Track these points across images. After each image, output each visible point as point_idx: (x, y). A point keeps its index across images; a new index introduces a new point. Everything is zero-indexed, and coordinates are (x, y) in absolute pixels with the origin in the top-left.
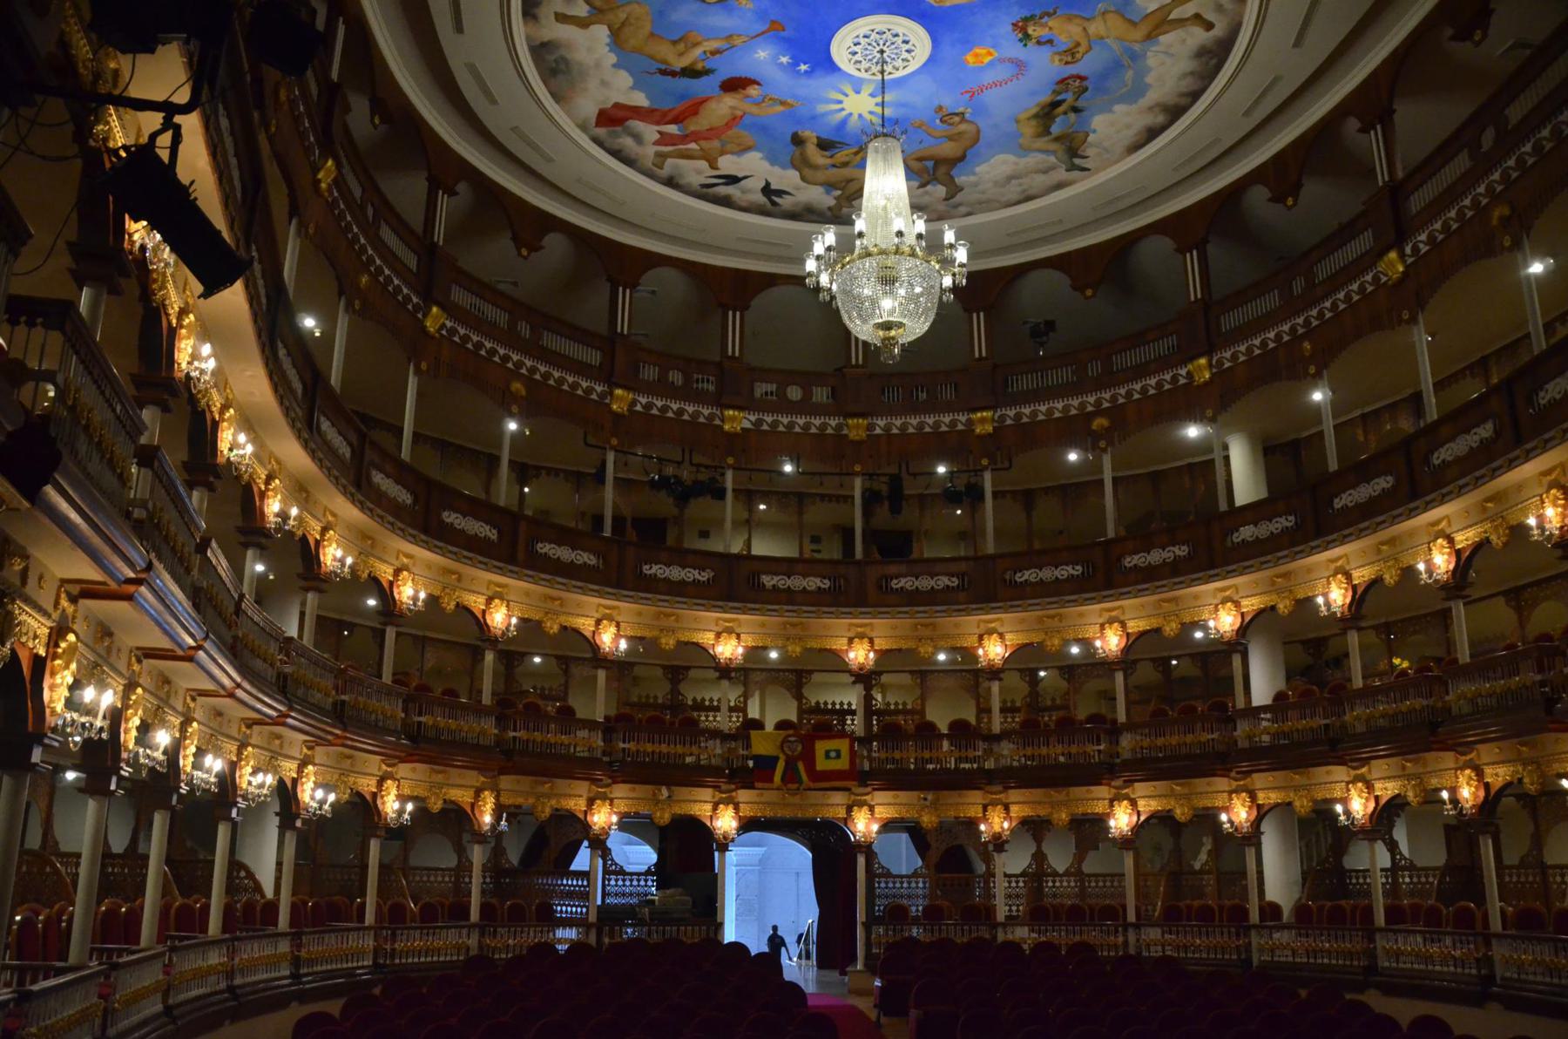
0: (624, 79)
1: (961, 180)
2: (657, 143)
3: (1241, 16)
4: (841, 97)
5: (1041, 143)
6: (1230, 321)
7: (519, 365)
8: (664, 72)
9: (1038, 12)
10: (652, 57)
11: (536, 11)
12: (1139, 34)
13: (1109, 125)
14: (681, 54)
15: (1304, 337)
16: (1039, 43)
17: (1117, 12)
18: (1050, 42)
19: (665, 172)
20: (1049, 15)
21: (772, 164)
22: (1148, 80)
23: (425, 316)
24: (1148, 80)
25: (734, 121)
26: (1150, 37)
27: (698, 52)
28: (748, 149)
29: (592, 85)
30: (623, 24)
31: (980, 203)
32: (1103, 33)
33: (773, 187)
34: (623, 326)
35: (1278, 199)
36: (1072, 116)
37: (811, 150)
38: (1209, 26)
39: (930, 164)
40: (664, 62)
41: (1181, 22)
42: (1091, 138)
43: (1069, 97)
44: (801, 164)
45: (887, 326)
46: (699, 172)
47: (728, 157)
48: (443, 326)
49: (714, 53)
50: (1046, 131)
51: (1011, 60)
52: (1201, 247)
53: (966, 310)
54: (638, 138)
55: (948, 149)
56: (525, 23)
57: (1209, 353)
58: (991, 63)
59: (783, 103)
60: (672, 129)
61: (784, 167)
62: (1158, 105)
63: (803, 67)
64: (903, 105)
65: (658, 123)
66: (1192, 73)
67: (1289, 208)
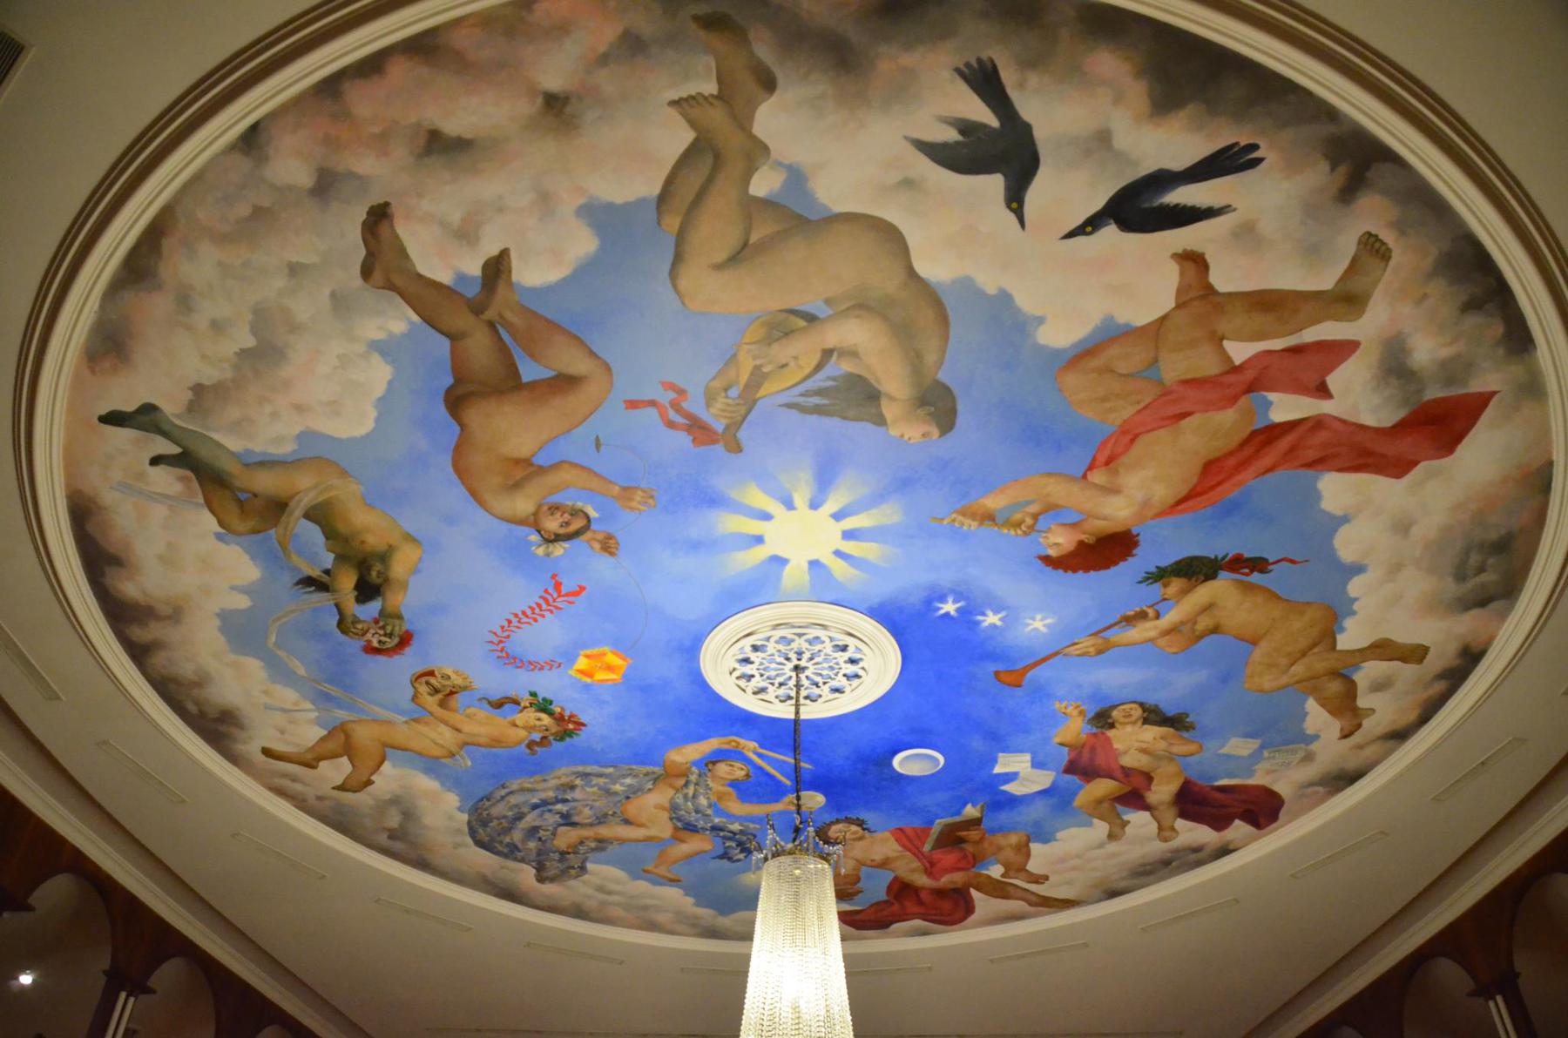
2: (1342, 350)
4: (850, 547)
9: (557, 746)
10: (1273, 596)
14: (1208, 608)
17: (437, 758)
19: (1372, 214)
25: (1110, 456)
27: (1172, 617)
28: (1084, 355)
29: (1429, 525)
30: (1304, 654)
33: (993, 185)
37: (894, 381)
39: (530, 371)
40: (1250, 588)
42: (209, 522)
44: (919, 309)
46: (1247, 234)
47: (1142, 317)
49: (1142, 616)
50: (321, 515)
54: (1395, 366)
55: (514, 430)
59: (989, 517)
60: (1284, 407)
61: (966, 285)
63: (950, 607)
64: (696, 546)
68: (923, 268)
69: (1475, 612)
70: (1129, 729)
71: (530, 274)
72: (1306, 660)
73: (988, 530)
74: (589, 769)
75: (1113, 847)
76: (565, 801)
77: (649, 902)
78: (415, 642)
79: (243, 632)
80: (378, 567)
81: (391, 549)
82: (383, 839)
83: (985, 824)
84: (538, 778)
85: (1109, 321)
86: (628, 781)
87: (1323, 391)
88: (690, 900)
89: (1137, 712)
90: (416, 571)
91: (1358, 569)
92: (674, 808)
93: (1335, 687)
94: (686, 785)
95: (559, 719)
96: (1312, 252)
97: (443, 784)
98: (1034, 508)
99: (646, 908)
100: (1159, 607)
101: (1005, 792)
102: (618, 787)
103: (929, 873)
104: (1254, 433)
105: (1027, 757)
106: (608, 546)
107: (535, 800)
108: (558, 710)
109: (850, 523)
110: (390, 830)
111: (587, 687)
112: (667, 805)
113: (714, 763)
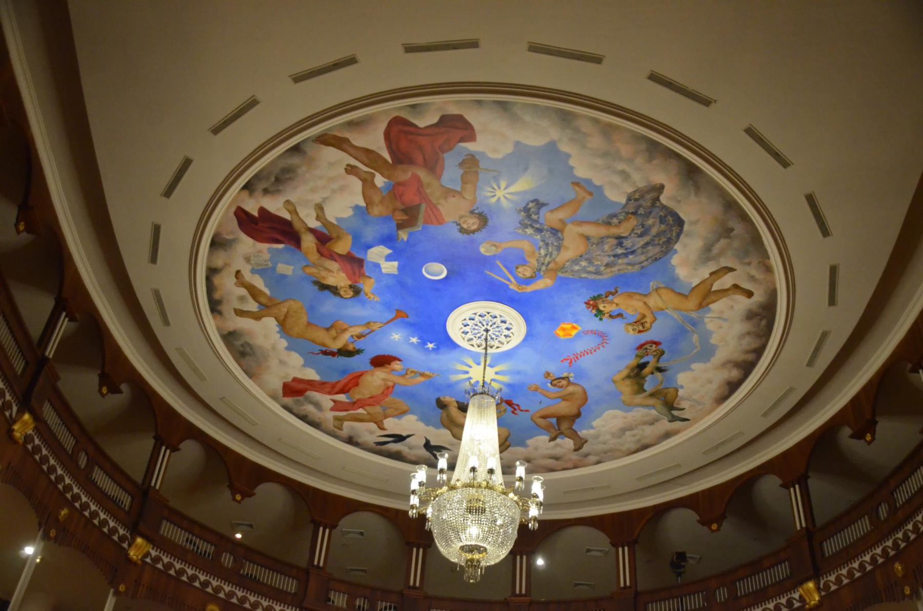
0: (296, 360)
1: (583, 433)
2: (332, 409)
3: (774, 284)
4: (467, 369)
5: (639, 399)
6: (831, 547)
7: (218, 590)
8: (325, 353)
9: (603, 292)
11: (219, 308)
12: (692, 303)
13: (694, 381)
14: (335, 338)
15: (895, 558)
16: (611, 316)
17: (665, 288)
18: (620, 315)
20: (613, 294)
21: (427, 424)
22: (713, 340)
23: (130, 545)
24: (713, 340)
25: (388, 390)
26: (702, 305)
27: (346, 337)
29: (273, 363)
31: (606, 452)
32: (661, 305)
34: (319, 559)
35: (852, 436)
36: (658, 375)
38: (750, 294)
39: (554, 420)
40: (324, 345)
41: (723, 292)
43: (650, 359)
45: (471, 549)
46: (372, 433)
48: (148, 554)
50: (641, 390)
51: (594, 332)
52: (802, 481)
53: (615, 545)
54: (317, 405)
55: (564, 408)
56: (214, 318)
57: (816, 575)
58: (578, 336)
59: (422, 375)
60: (342, 397)
61: (437, 427)
62: (729, 362)
63: (430, 346)
64: (518, 373)
65: (330, 393)
66: (748, 333)
67: (869, 443)
68: (448, 432)
69: (231, 329)
70: (342, 284)
71: (546, 438)
72: (283, 314)
73: (422, 371)
74: (593, 277)
75: (317, 198)
76: (615, 256)
77: (599, 161)
78: (638, 345)
79: (706, 352)
80: (632, 374)
81: (623, 379)
82: (739, 228)
83: (393, 225)
84: (622, 272)
85: (399, 419)
86: (577, 268)
87: (334, 401)
88: (572, 162)
89: (342, 293)
90: (620, 371)
91: (287, 349)
92: (559, 248)
93: (263, 300)
94: (549, 263)
95: (595, 307)
96: (352, 428)
97: (674, 270)
98: (408, 376)
99: (605, 155)
100: (352, 340)
101: (390, 248)
102: (584, 264)
103: (419, 180)
104: (348, 391)
105: (384, 271)
106: (548, 374)
107: (631, 257)
108: (594, 312)
109: (466, 376)
110: (728, 237)
111: (576, 322)
112: (562, 250)
113: (531, 277)
